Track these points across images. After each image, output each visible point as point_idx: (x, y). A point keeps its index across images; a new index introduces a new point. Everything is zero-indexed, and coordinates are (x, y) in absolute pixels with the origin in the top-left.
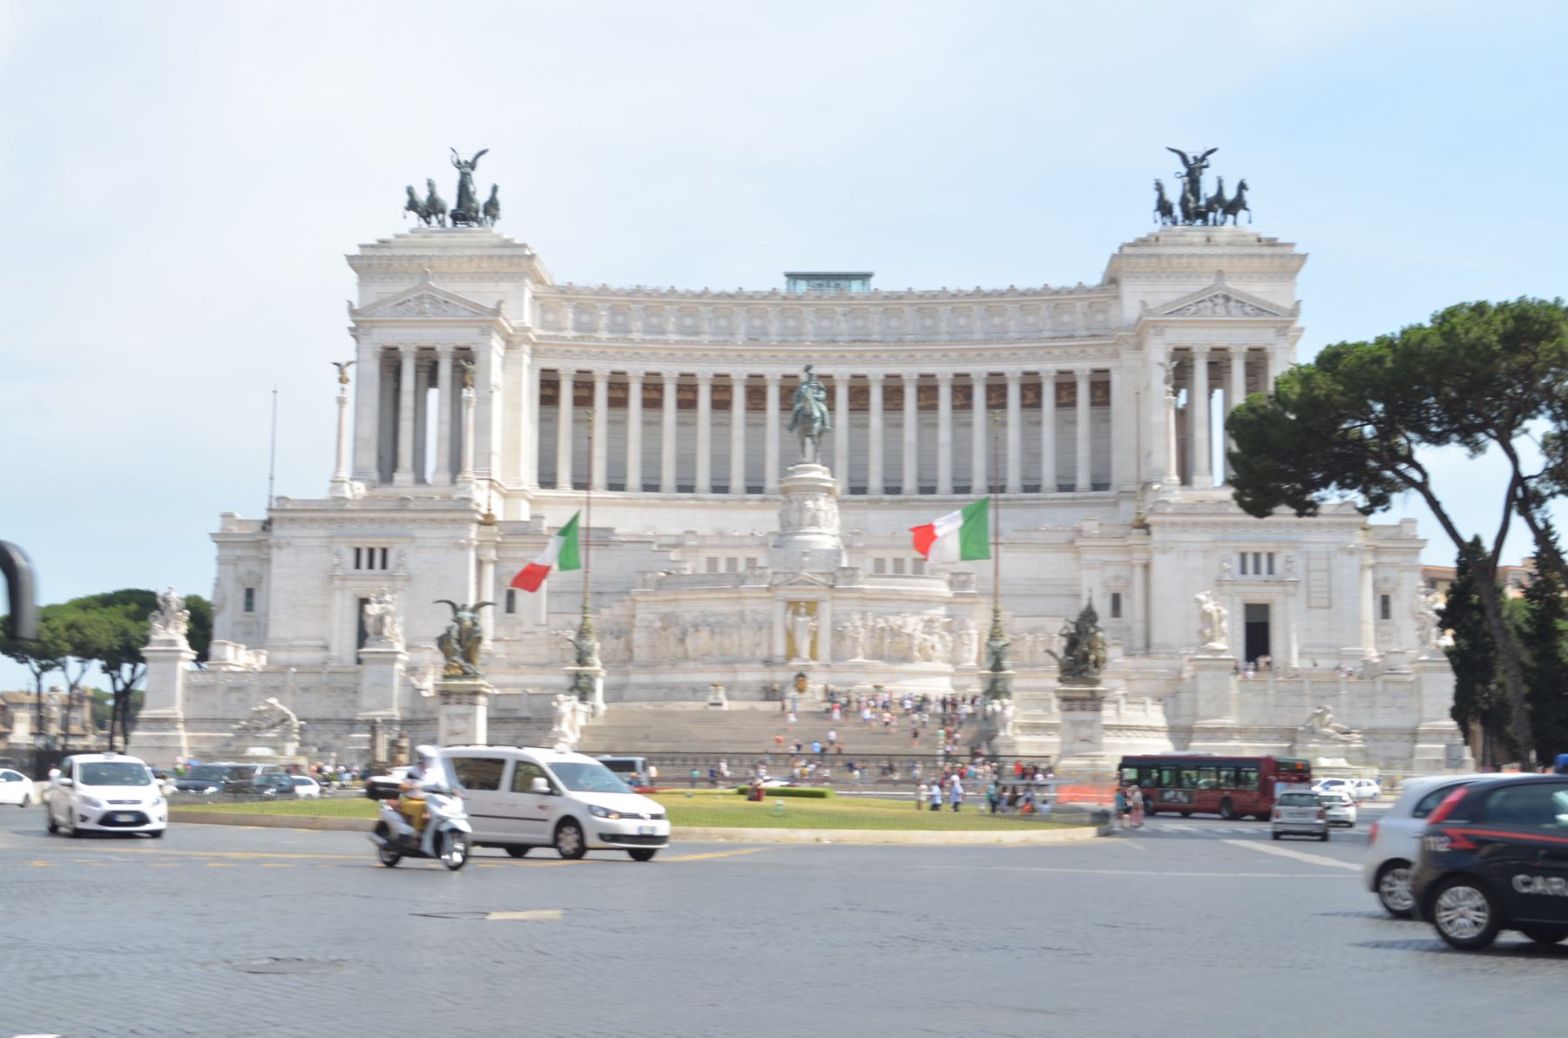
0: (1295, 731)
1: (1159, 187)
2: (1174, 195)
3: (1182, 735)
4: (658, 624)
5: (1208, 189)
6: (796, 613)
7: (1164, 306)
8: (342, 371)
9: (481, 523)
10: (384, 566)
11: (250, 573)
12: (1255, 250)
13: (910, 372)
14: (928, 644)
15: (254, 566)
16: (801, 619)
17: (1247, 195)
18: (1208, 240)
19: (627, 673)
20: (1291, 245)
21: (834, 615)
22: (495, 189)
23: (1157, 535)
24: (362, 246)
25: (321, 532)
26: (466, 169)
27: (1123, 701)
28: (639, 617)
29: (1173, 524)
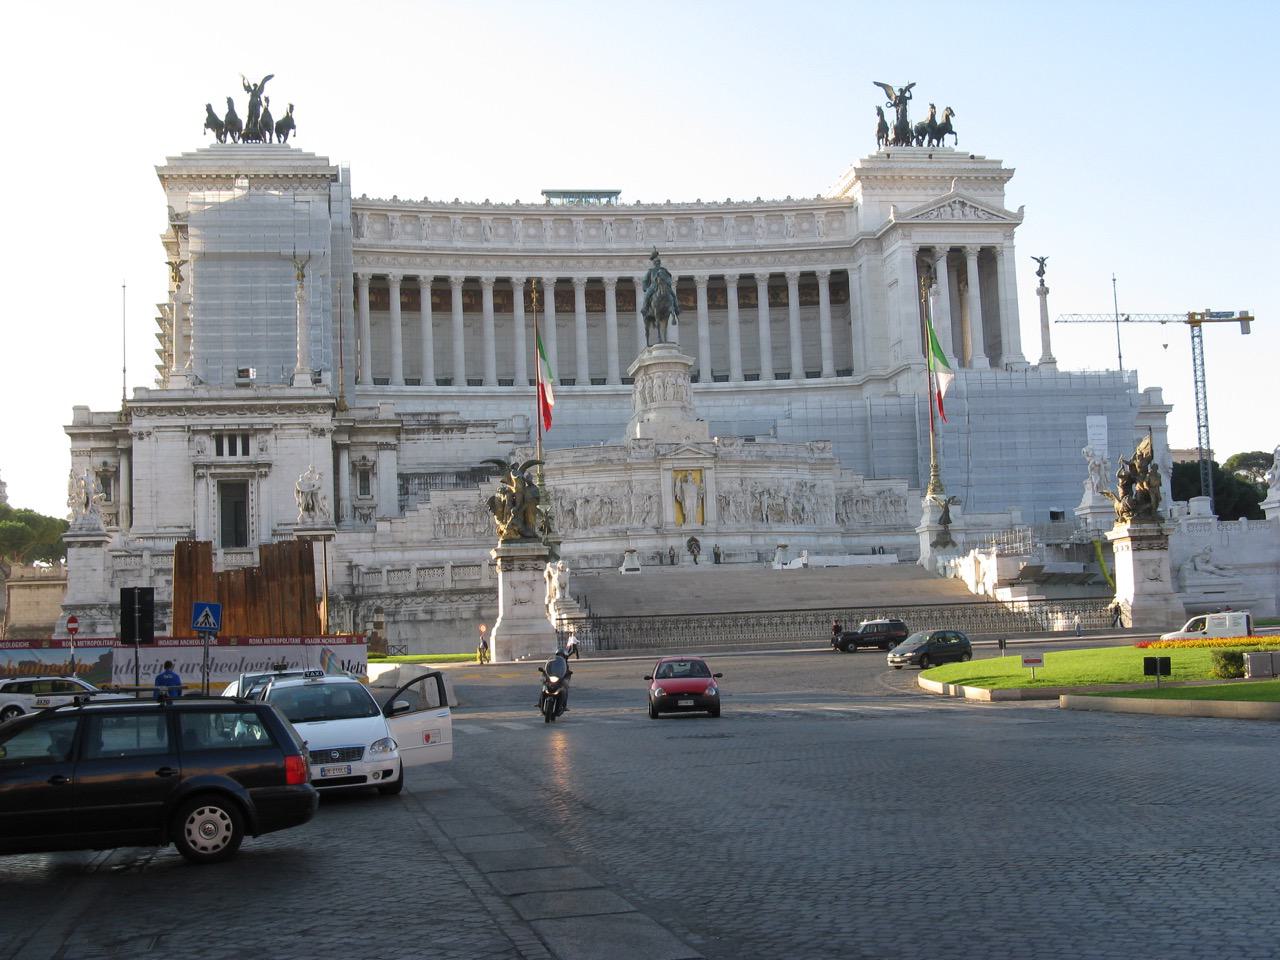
1: (880, 112)
7: (912, 212)
10: (246, 452)
11: (105, 464)
12: (971, 166)
14: (799, 507)
15: (111, 460)
18: (930, 156)
20: (1000, 162)
22: (292, 107)
25: (181, 421)
26: (256, 92)
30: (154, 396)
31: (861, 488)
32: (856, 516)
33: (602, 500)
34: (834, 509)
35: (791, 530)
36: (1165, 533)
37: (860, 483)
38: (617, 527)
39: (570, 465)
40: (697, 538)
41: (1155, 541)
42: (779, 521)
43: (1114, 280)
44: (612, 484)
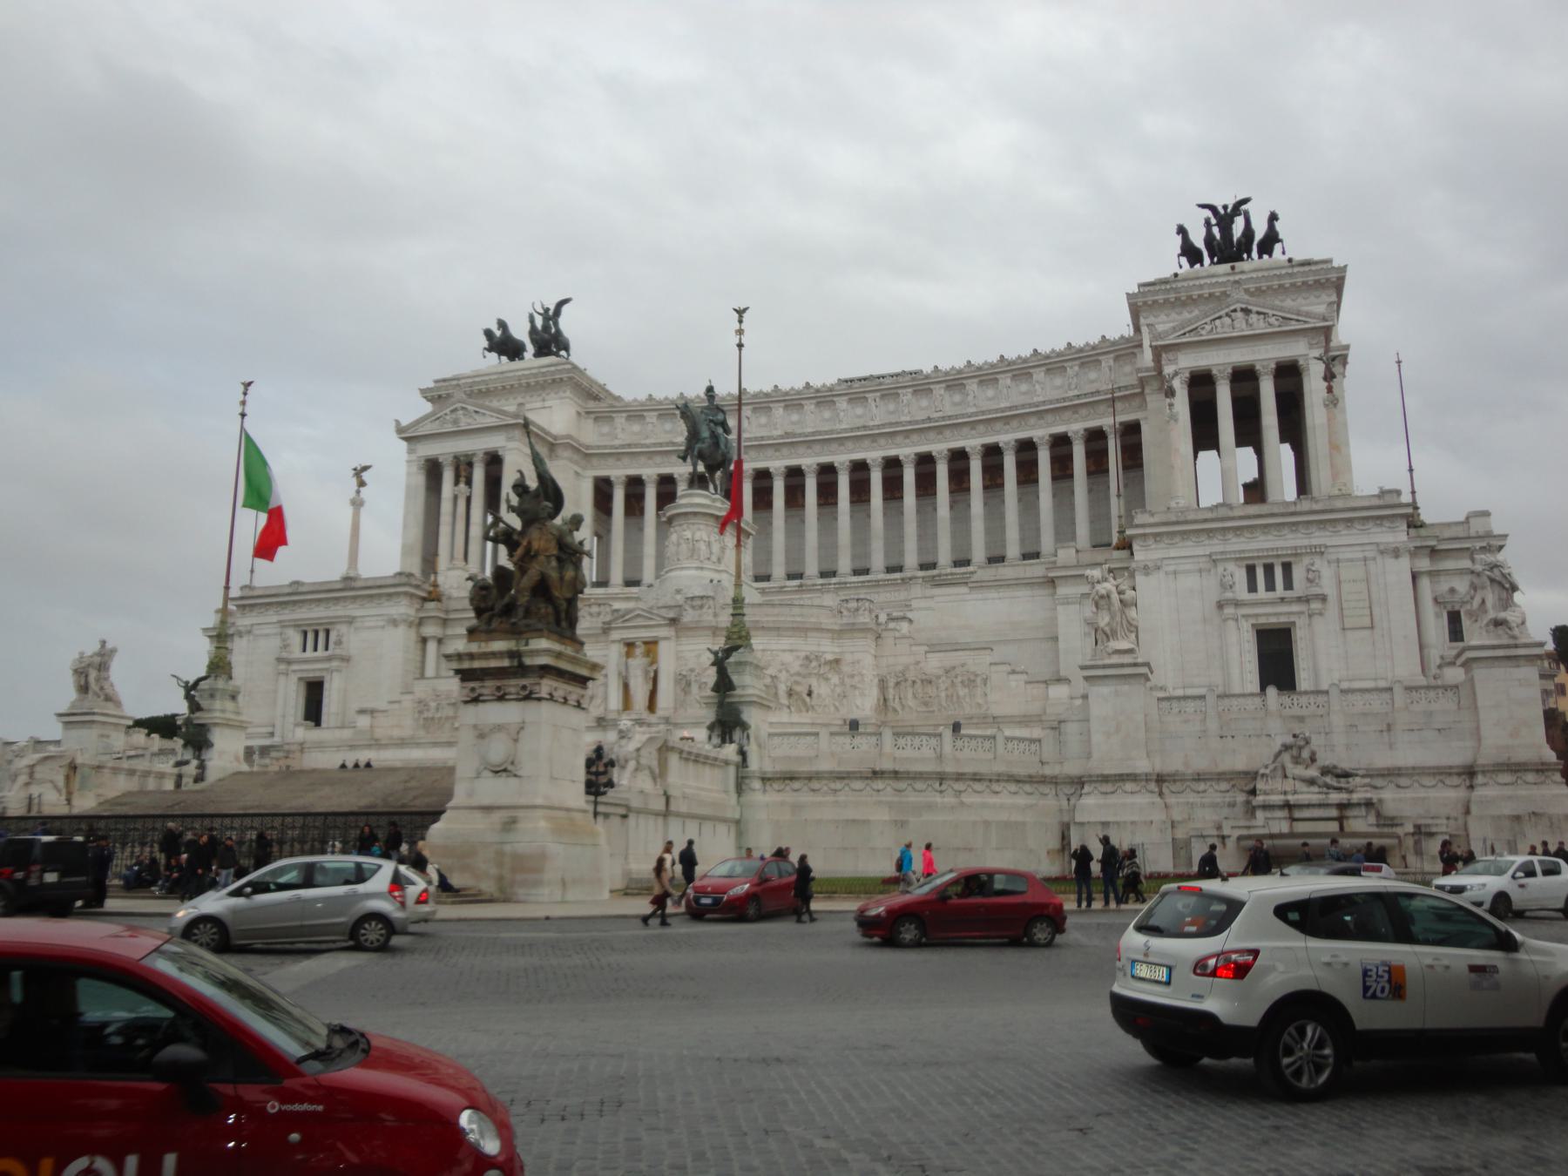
0: (1253, 775)
1: (1182, 230)
2: (1198, 240)
3: (1068, 790)
6: (628, 655)
7: (1174, 329)
8: (359, 472)
9: (425, 600)
13: (939, 447)
14: (802, 689)
17: (1278, 225)
20: (1329, 261)
21: (678, 658)
23: (1140, 554)
24: (436, 381)
27: (948, 734)
29: (1156, 535)
30: (256, 593)
32: (911, 702)
36: (528, 661)
41: (513, 682)
43: (1399, 362)
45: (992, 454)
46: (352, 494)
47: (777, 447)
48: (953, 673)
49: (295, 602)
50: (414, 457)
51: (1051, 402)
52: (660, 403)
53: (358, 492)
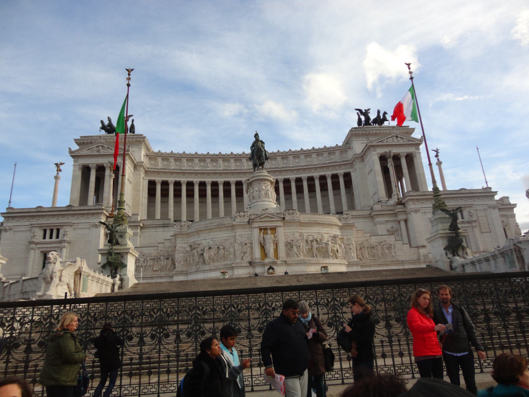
4: (188, 249)
5: (373, 116)
7: (376, 140)
9: (107, 217)
10: (57, 237)
14: (335, 249)
16: (268, 236)
19: (172, 277)
20: (408, 126)
21: (285, 235)
22: (133, 121)
23: (411, 206)
24: (81, 137)
25: (28, 223)
28: (178, 246)
29: (417, 200)
31: (369, 241)
32: (367, 256)
33: (218, 247)
34: (355, 251)
35: (331, 262)
37: (368, 238)
38: (228, 262)
39: (203, 229)
40: (274, 267)
42: (324, 257)
44: (224, 238)
45: (299, 181)
46: (55, 174)
47: (221, 174)
48: (381, 244)
49: (39, 216)
50: (77, 164)
51: (320, 164)
52: (175, 154)
53: (58, 173)
